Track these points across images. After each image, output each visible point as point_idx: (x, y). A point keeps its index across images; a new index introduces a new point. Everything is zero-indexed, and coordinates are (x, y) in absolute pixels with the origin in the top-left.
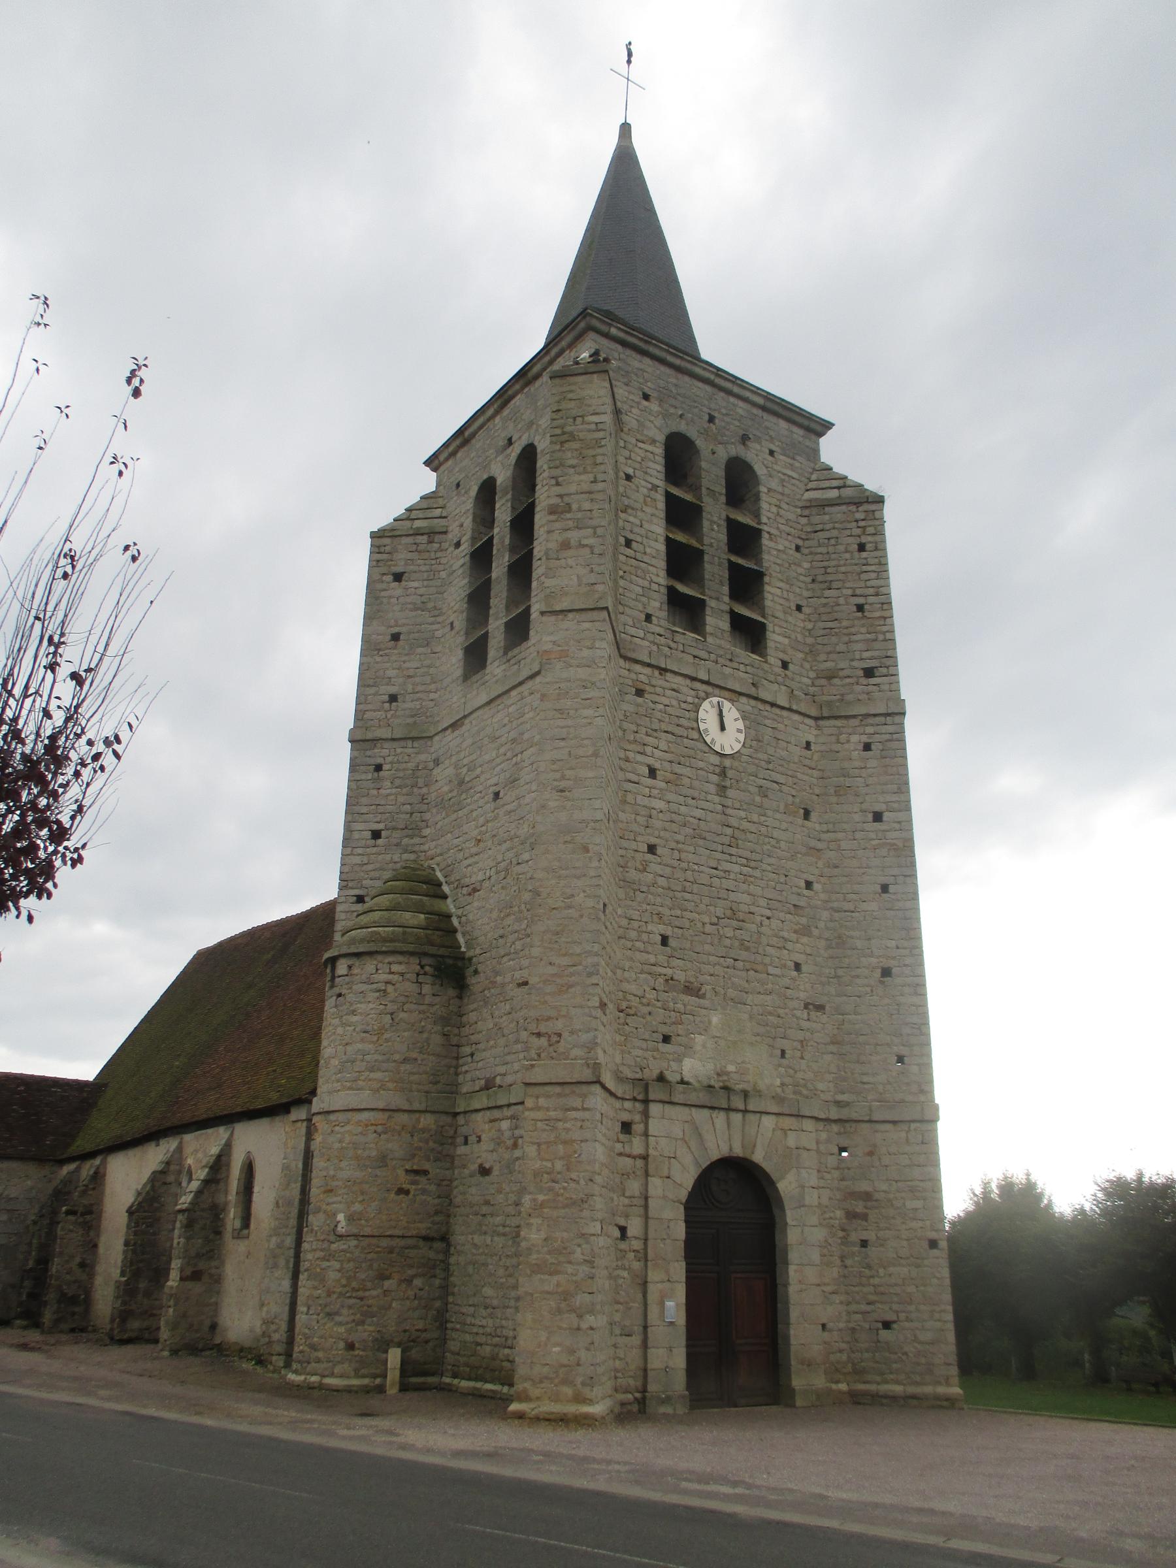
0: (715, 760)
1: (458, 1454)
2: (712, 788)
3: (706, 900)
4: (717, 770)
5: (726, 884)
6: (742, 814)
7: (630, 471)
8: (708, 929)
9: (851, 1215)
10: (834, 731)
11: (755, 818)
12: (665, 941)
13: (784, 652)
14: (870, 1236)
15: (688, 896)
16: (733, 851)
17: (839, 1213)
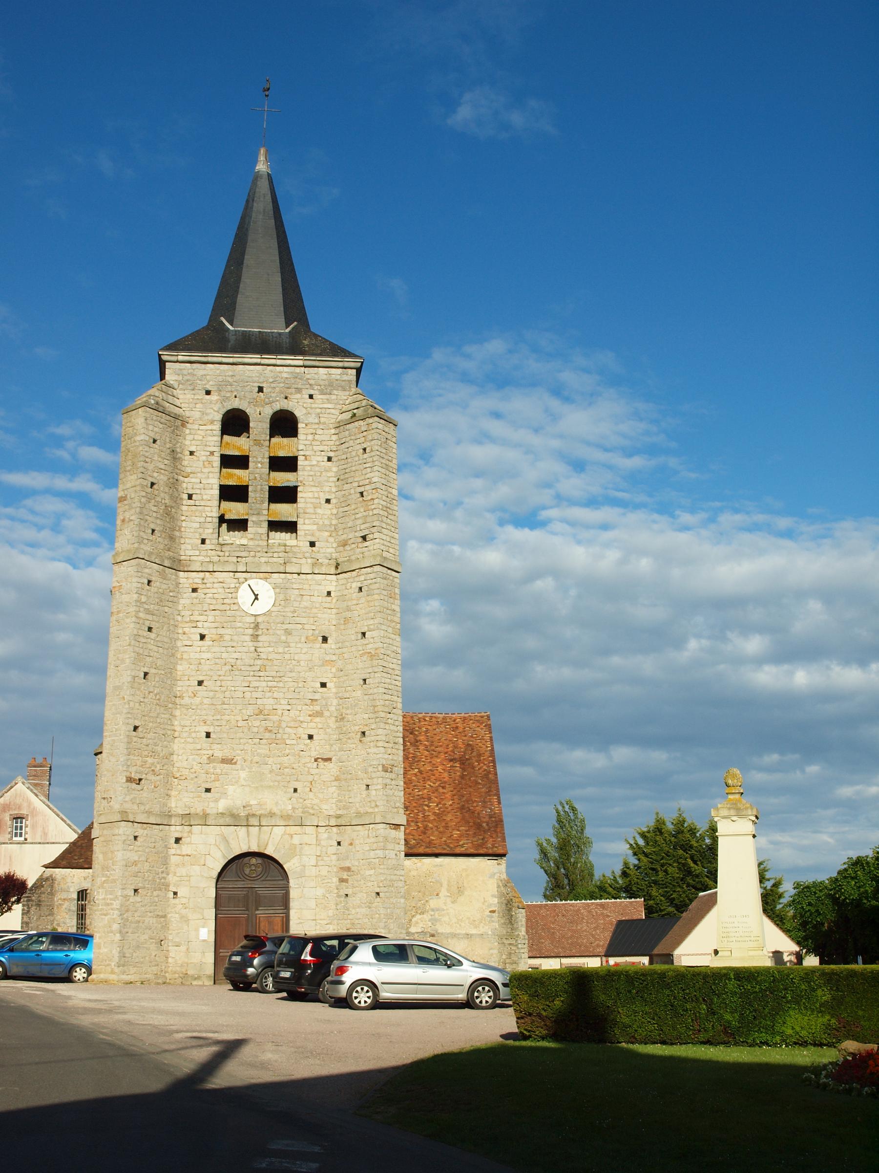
0: (252, 619)
1: (85, 1000)
2: (248, 638)
3: (239, 707)
4: (252, 626)
5: (255, 695)
6: (271, 649)
7: (193, 449)
8: (240, 724)
9: (342, 880)
10: (344, 582)
11: (281, 650)
12: (208, 735)
13: (313, 535)
14: (349, 893)
15: (225, 706)
16: (261, 674)
17: (335, 880)
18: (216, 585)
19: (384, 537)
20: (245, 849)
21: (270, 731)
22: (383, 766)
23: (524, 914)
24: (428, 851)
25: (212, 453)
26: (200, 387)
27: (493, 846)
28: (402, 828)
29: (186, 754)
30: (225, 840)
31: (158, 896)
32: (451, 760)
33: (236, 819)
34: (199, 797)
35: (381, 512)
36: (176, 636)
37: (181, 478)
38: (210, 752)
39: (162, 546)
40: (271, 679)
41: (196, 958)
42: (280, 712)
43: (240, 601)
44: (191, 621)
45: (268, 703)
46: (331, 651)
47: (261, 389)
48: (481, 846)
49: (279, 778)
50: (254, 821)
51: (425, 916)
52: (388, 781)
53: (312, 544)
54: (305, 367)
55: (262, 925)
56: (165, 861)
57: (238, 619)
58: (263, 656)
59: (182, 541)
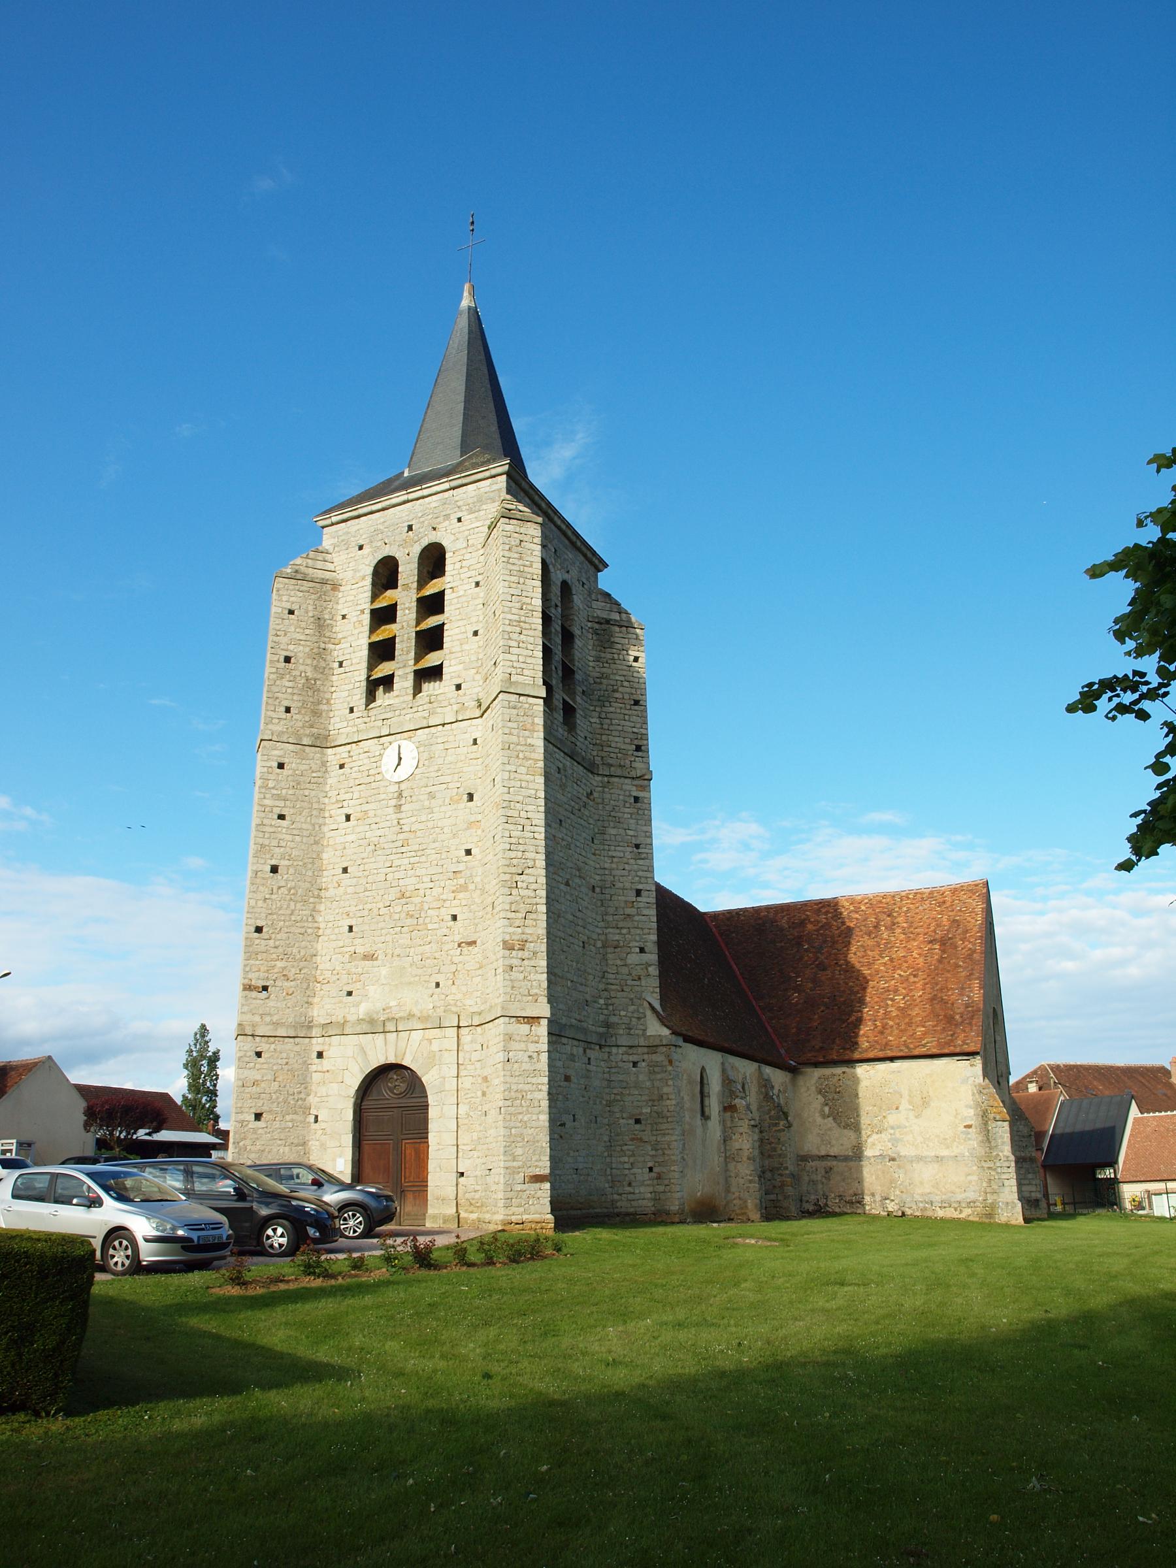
2: (391, 810)
5: (397, 875)
6: (413, 819)
12: (351, 929)
15: (367, 893)
18: (362, 756)
19: (514, 658)
20: (382, 1061)
21: (412, 916)
22: (505, 942)
23: (1008, 1128)
24: (881, 1054)
25: (363, 612)
26: (353, 544)
27: (964, 1043)
28: (545, 1022)
29: (330, 954)
30: (363, 1050)
31: (292, 1121)
32: (931, 942)
33: (375, 1026)
34: (341, 1002)
35: (509, 629)
36: (321, 821)
37: (331, 646)
38: (352, 949)
39: (301, 724)
40: (413, 854)
42: (421, 892)
43: (383, 769)
44: (337, 801)
45: (410, 883)
46: (476, 810)
47: (410, 528)
48: (948, 1044)
49: (420, 971)
50: (390, 1026)
51: (883, 1135)
52: (515, 962)
53: (458, 687)
54: (454, 488)
55: (408, 1152)
56: (305, 1083)
57: (382, 790)
58: (405, 828)
59: (331, 714)
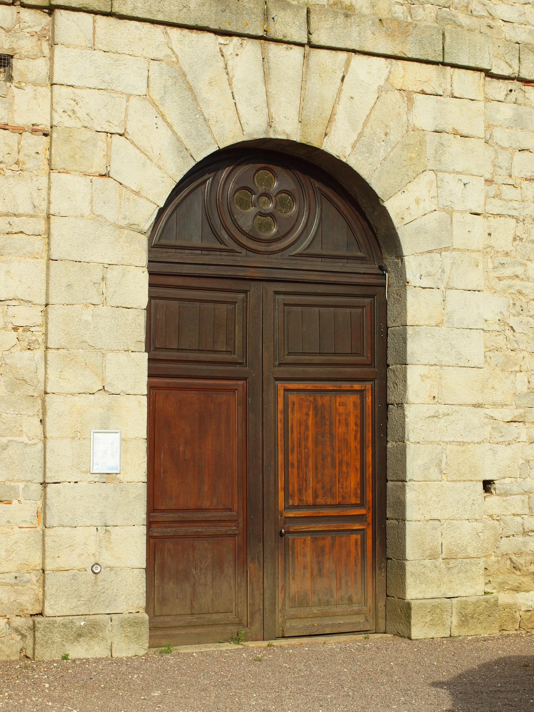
41: (75, 547)
55: (295, 417)
